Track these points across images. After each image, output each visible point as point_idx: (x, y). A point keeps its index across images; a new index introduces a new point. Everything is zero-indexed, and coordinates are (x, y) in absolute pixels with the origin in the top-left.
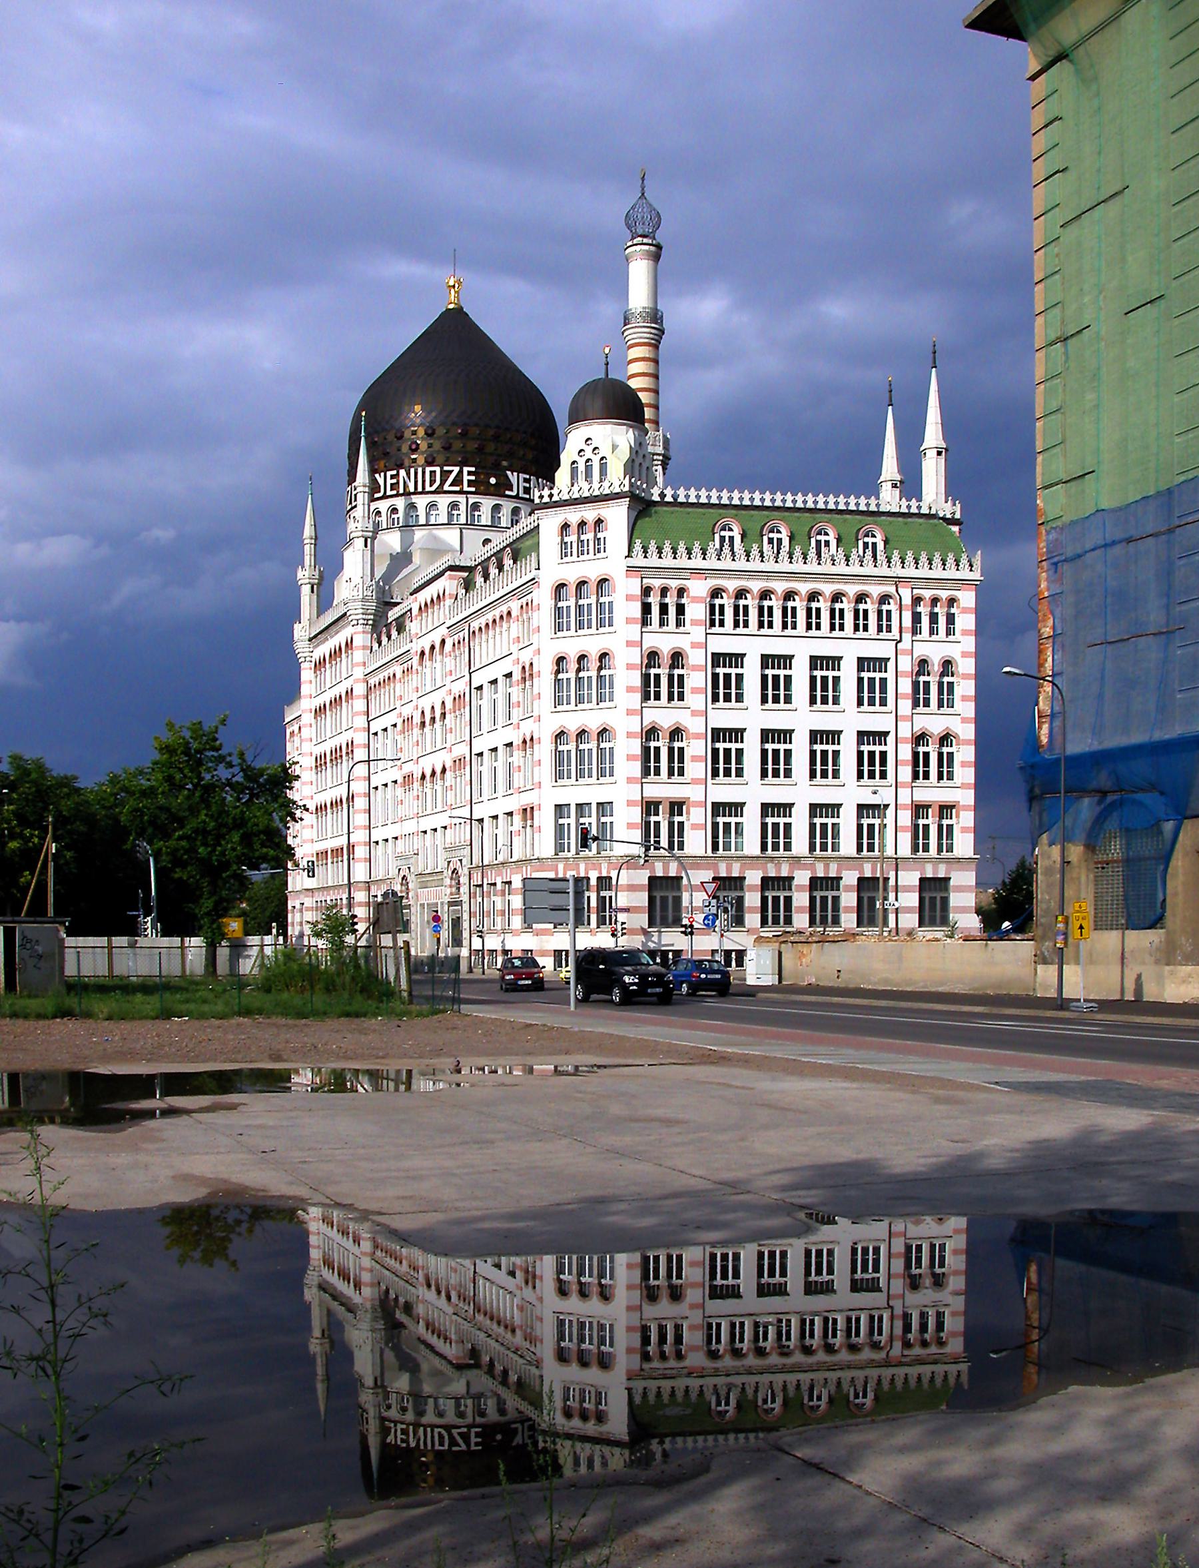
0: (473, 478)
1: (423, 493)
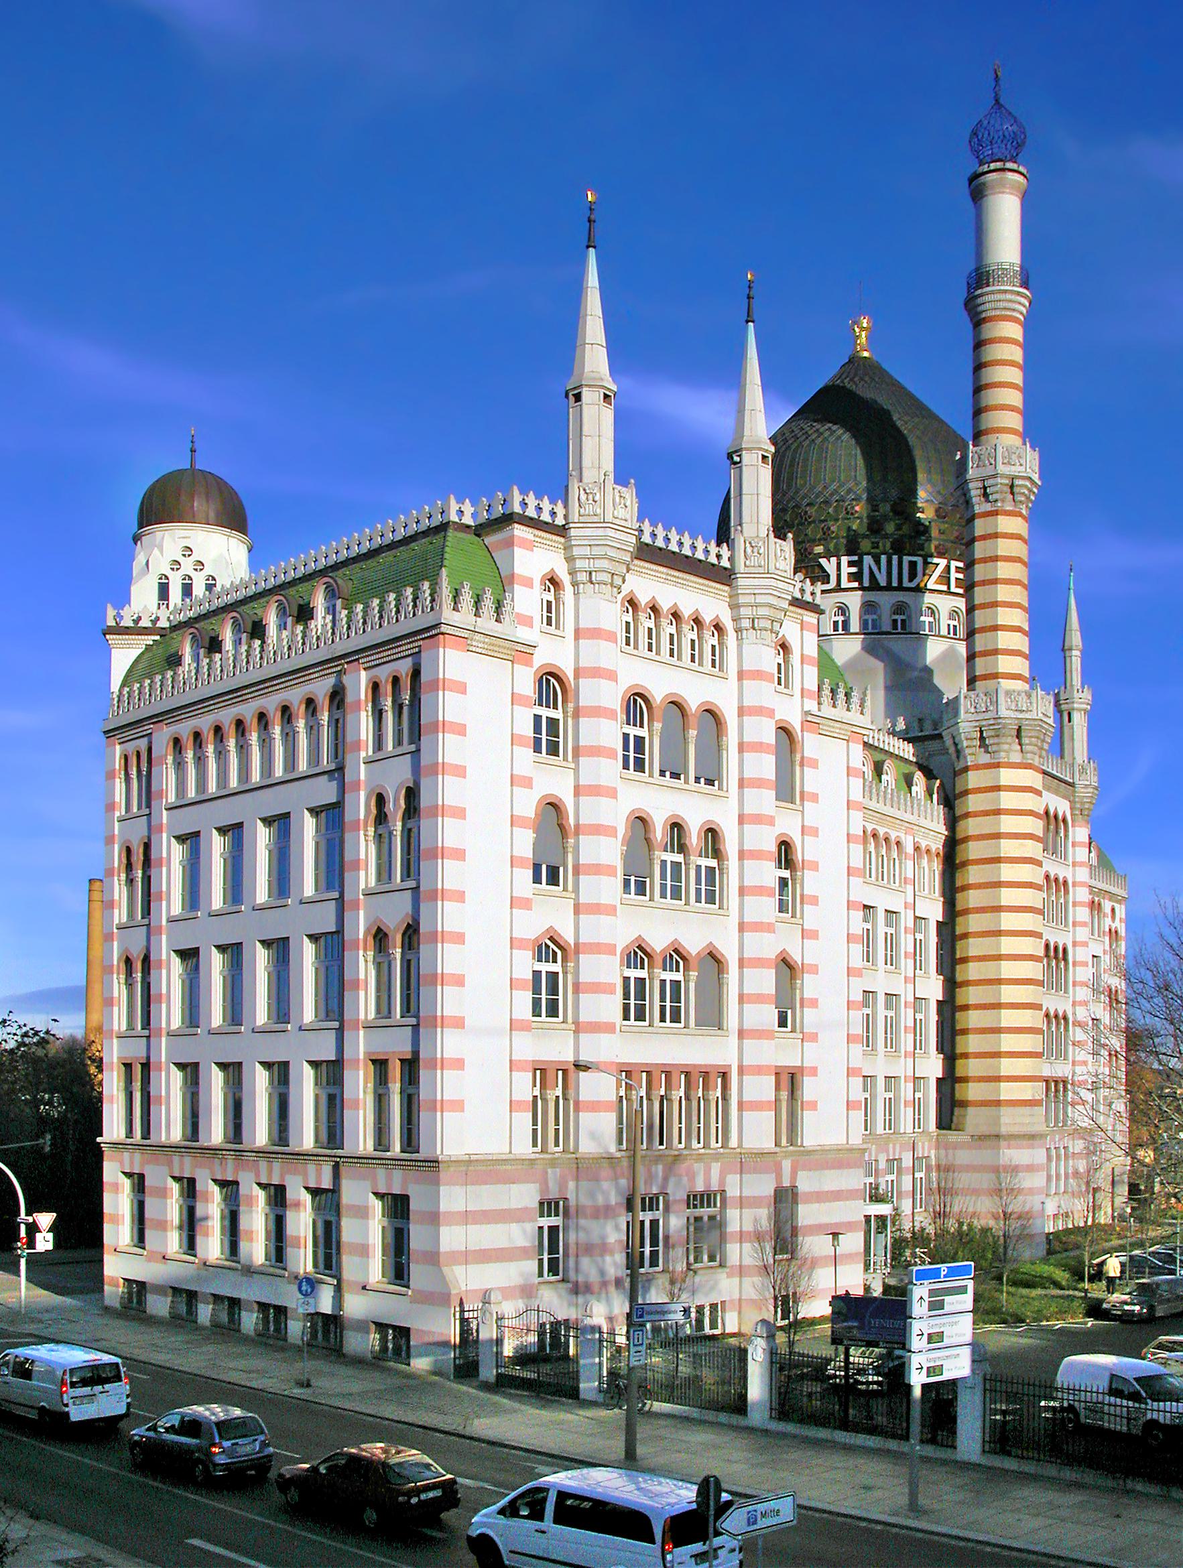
0: (961, 576)
1: (900, 588)
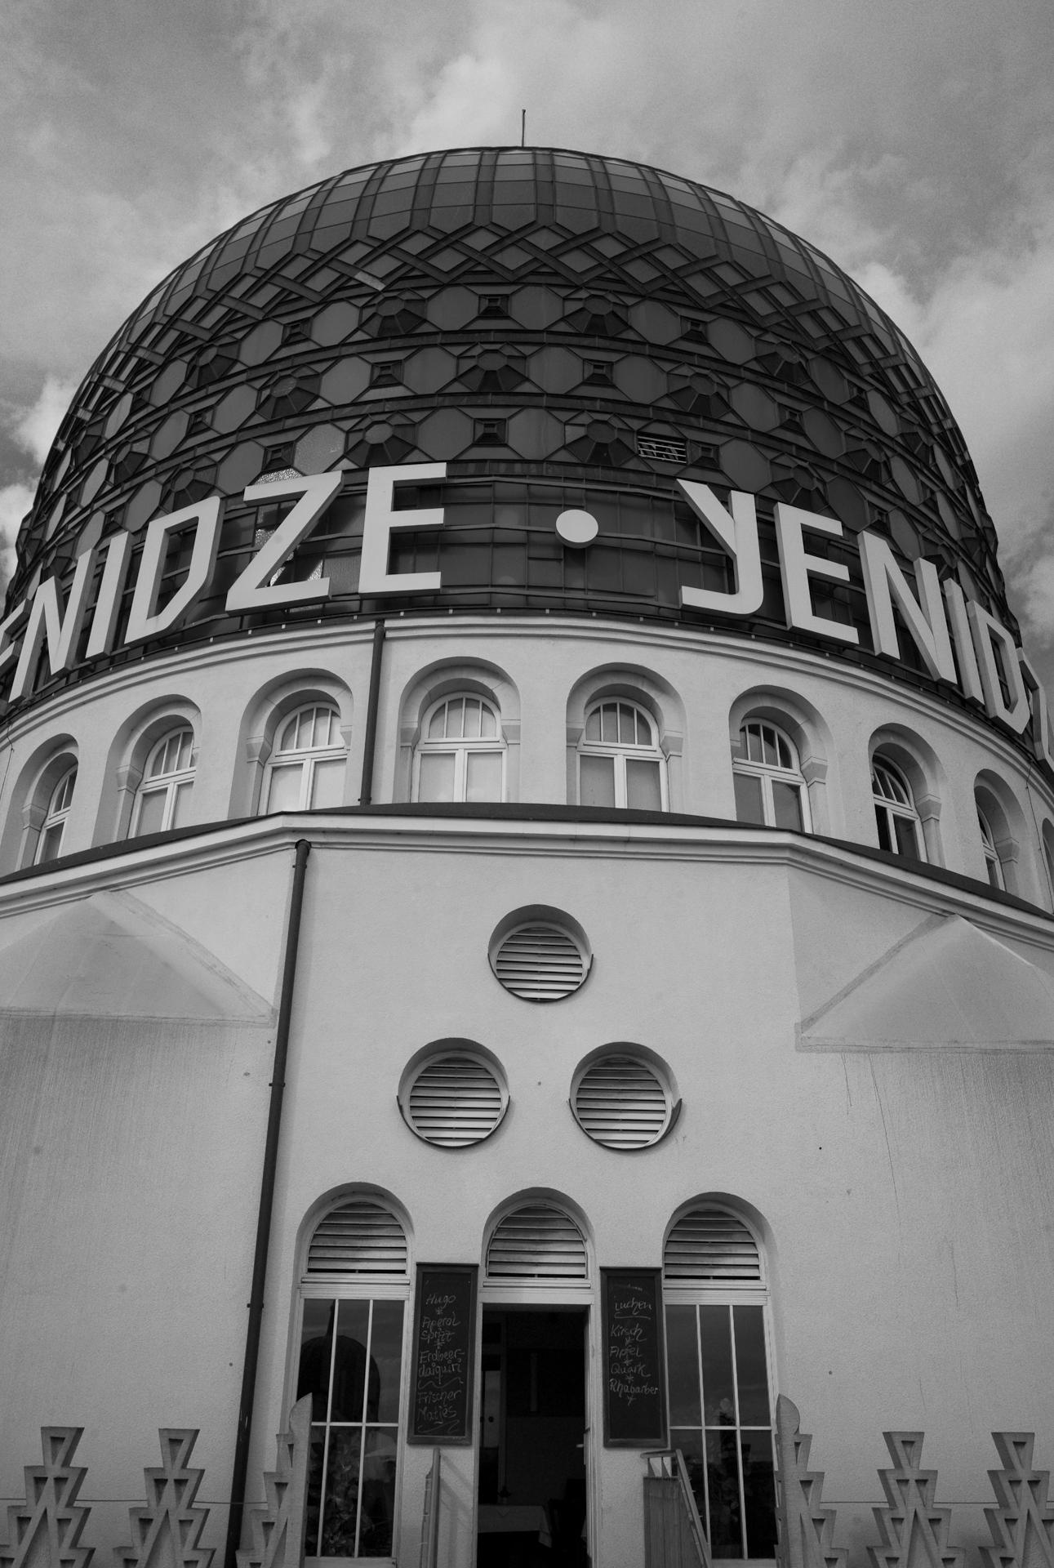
0: (433, 516)
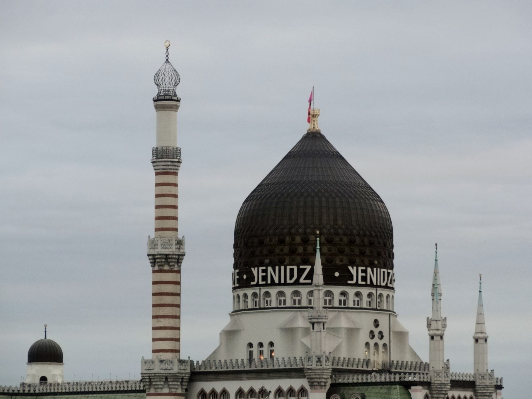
1: (286, 284)
